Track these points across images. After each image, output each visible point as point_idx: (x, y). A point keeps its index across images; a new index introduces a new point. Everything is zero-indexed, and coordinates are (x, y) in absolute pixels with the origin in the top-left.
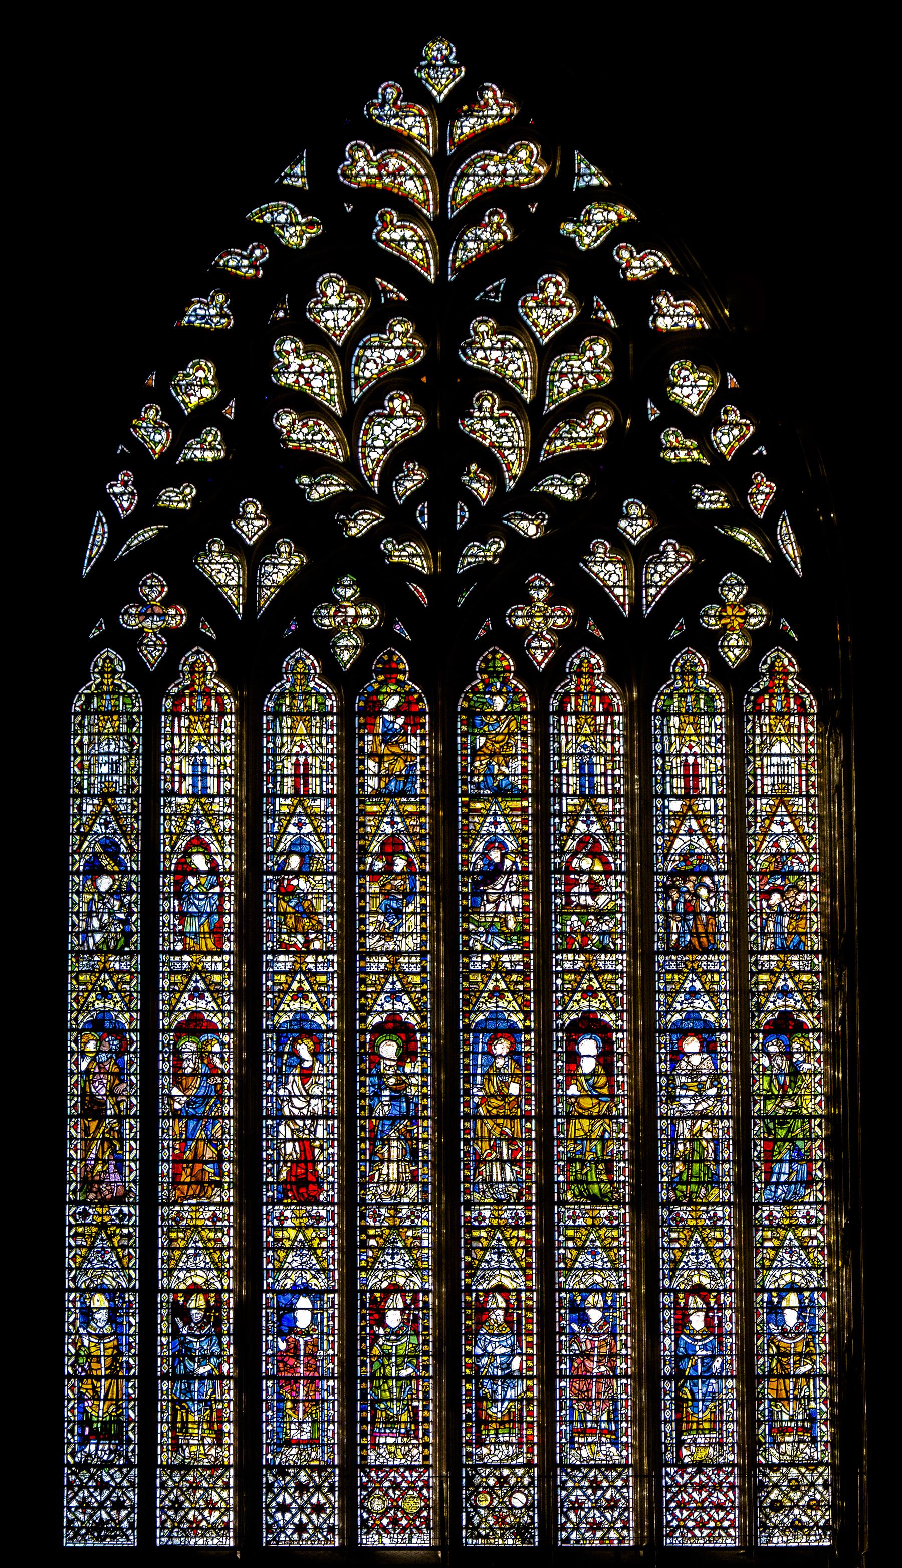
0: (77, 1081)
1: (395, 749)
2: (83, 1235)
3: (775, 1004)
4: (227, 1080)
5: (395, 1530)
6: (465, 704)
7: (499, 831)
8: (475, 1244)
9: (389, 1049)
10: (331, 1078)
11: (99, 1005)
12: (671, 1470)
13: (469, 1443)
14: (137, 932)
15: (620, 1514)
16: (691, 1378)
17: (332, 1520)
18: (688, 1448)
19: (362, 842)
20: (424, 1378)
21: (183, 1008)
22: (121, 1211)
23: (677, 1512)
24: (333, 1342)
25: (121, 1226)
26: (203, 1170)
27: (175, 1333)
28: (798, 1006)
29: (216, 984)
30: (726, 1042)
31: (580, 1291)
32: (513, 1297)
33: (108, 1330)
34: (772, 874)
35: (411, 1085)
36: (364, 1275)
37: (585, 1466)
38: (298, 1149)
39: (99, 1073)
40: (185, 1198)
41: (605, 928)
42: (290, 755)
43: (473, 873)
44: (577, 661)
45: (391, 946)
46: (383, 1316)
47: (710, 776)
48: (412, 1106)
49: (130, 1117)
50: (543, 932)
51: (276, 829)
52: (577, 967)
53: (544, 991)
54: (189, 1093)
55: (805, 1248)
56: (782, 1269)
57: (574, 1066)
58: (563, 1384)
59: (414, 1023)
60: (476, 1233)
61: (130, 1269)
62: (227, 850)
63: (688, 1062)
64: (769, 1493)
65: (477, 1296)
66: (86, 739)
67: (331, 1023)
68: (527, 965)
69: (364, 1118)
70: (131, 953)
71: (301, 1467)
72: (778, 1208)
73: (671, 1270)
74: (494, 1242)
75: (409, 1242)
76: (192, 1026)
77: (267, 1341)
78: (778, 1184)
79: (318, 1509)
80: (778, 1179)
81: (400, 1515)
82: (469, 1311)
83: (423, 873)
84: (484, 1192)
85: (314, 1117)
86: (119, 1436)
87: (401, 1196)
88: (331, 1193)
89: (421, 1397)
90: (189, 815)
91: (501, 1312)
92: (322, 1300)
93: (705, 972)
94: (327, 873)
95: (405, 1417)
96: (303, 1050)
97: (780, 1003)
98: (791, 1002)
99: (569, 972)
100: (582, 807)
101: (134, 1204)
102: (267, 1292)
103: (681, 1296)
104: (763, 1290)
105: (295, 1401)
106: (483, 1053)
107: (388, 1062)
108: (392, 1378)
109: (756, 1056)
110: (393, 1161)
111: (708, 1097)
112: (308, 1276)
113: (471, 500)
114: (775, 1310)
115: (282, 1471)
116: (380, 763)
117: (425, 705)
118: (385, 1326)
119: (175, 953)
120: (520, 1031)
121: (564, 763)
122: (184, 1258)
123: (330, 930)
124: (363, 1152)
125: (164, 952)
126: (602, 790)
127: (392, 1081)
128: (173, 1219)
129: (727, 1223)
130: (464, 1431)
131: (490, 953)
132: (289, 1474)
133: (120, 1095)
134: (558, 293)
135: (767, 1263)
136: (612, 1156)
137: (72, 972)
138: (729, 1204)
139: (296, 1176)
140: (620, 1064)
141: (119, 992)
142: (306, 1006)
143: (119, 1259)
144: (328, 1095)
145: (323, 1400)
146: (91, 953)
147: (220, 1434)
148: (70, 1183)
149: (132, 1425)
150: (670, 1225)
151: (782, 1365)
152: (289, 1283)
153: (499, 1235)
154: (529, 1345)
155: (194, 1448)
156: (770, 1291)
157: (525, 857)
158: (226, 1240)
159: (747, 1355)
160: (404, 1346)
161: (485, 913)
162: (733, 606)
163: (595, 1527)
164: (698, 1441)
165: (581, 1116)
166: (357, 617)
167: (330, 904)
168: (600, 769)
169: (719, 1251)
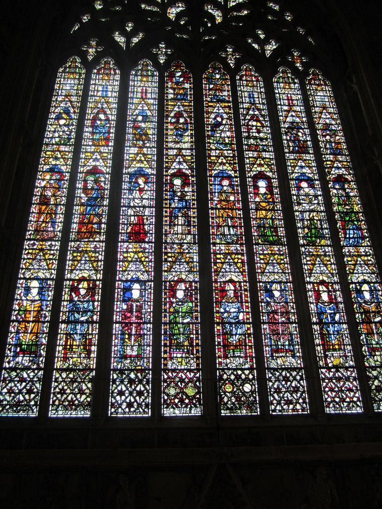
0: (39, 190)
2: (31, 254)
4: (106, 192)
5: (182, 406)
6: (205, 76)
7: (220, 111)
8: (218, 261)
9: (178, 182)
10: (152, 192)
11: (54, 163)
12: (324, 370)
13: (220, 357)
14: (73, 138)
15: (301, 395)
16: (326, 323)
17: (147, 400)
18: (330, 359)
19: (167, 113)
20: (195, 323)
21: (90, 164)
22: (51, 244)
23: (329, 393)
24: (150, 305)
25: (50, 250)
26: (92, 227)
27: (71, 300)
28: (344, 173)
29: (105, 157)
30: (318, 184)
31: (269, 282)
32: (237, 285)
33: (37, 298)
35: (187, 195)
36: (166, 274)
37: (280, 369)
38: (136, 219)
39: (50, 187)
40: (83, 239)
41: (264, 144)
42: (140, 86)
43: (211, 124)
44: (245, 67)
45: (178, 146)
46: (176, 293)
47: (297, 100)
48: (188, 204)
49: (60, 205)
50: (240, 144)
51: (133, 108)
52: (254, 156)
53: (242, 164)
54: (89, 196)
55: (367, 265)
56: (358, 273)
57: (256, 191)
58: (265, 326)
59: (188, 173)
60: (218, 256)
61: (51, 269)
62: (113, 113)
63: (304, 191)
64: (373, 382)
65: (221, 284)
67: (153, 172)
68: (234, 155)
69: (167, 208)
70: (70, 145)
71: (132, 370)
72: (351, 248)
73: (309, 273)
74: (227, 260)
75: (187, 259)
76: (93, 171)
77: (117, 305)
79: (140, 393)
80: (349, 236)
81: (184, 397)
82: (217, 291)
83: (191, 123)
84: (221, 239)
85: (144, 207)
86: (35, 353)
87: (183, 240)
89: (194, 333)
90: (100, 102)
91: (232, 292)
92: (145, 285)
93: (306, 160)
94: (153, 122)
95: (186, 343)
96: (141, 181)
97: (337, 171)
98: (341, 171)
99: (251, 157)
100: (251, 106)
101: (58, 241)
102: (118, 281)
104: (352, 283)
106: (218, 185)
107: (177, 187)
108: (179, 323)
109: (331, 189)
110: (180, 225)
111: (314, 204)
112: (139, 274)
114: (359, 292)
115: (121, 372)
116: (174, 91)
118: (176, 298)
119: (89, 145)
120: (233, 177)
121: (243, 94)
122: (79, 265)
123: (154, 140)
124: (166, 221)
125: (84, 145)
127: (179, 194)
128: (76, 248)
129: (331, 254)
130: (217, 350)
131: (219, 150)
132: (125, 374)
133: (58, 196)
135: (351, 271)
136: (277, 225)
137: (44, 150)
139: (135, 230)
140: (276, 191)
141: (64, 158)
142: (142, 165)
143: (48, 265)
144: (151, 198)
145: (144, 334)
146: (53, 144)
147: (89, 352)
148: (29, 231)
149: (43, 347)
150: (306, 254)
151: (368, 318)
152: (129, 277)
153: (229, 257)
154: (247, 307)
155: (75, 359)
156: (355, 283)
157: (231, 120)
158: (100, 257)
159: (350, 312)
160: (184, 308)
161: (216, 137)
163: (289, 402)
164: (334, 355)
165: (262, 210)
167: (154, 132)
169: (329, 266)
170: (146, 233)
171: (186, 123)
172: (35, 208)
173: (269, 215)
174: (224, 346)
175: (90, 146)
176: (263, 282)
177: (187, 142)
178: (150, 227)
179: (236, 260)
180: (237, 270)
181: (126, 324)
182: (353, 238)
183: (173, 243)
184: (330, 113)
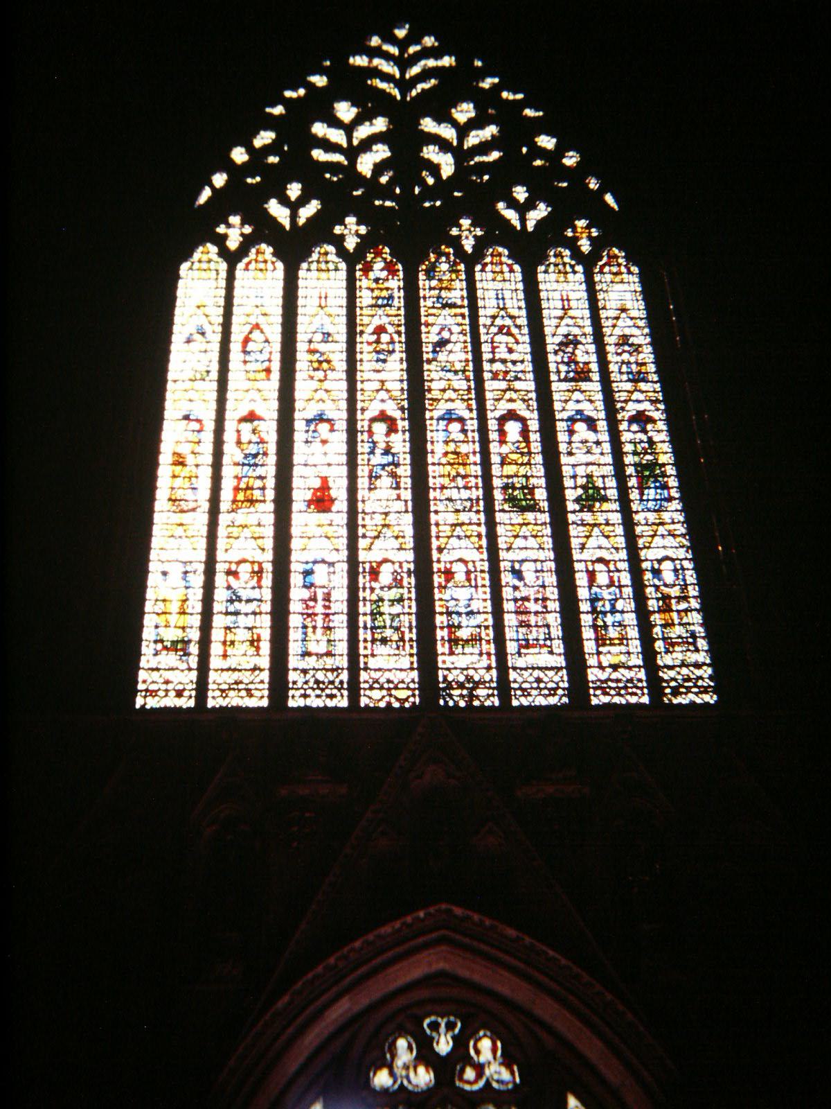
1: (381, 286)
3: (632, 408)
9: (380, 428)
13: (443, 654)
16: (601, 612)
20: (409, 614)
27: (229, 587)
31: (518, 561)
32: (470, 566)
48: (396, 459)
68: (469, 387)
74: (455, 534)
76: (249, 418)
78: (648, 500)
88: (341, 505)
103: (589, 563)
106: (443, 430)
113: (423, 183)
114: (657, 573)
115: (305, 672)
117: (400, 267)
127: (382, 445)
135: (647, 545)
138: (616, 511)
147: (258, 648)
149: (193, 643)
151: (666, 604)
156: (652, 561)
157: (465, 335)
160: (394, 594)
165: (510, 464)
170: (332, 501)
171: (392, 342)
173: (522, 470)
174: (450, 641)
177: (395, 368)
178: (339, 491)
180: (472, 546)
181: (309, 615)
182: (655, 500)
183: (374, 513)
184: (632, 318)
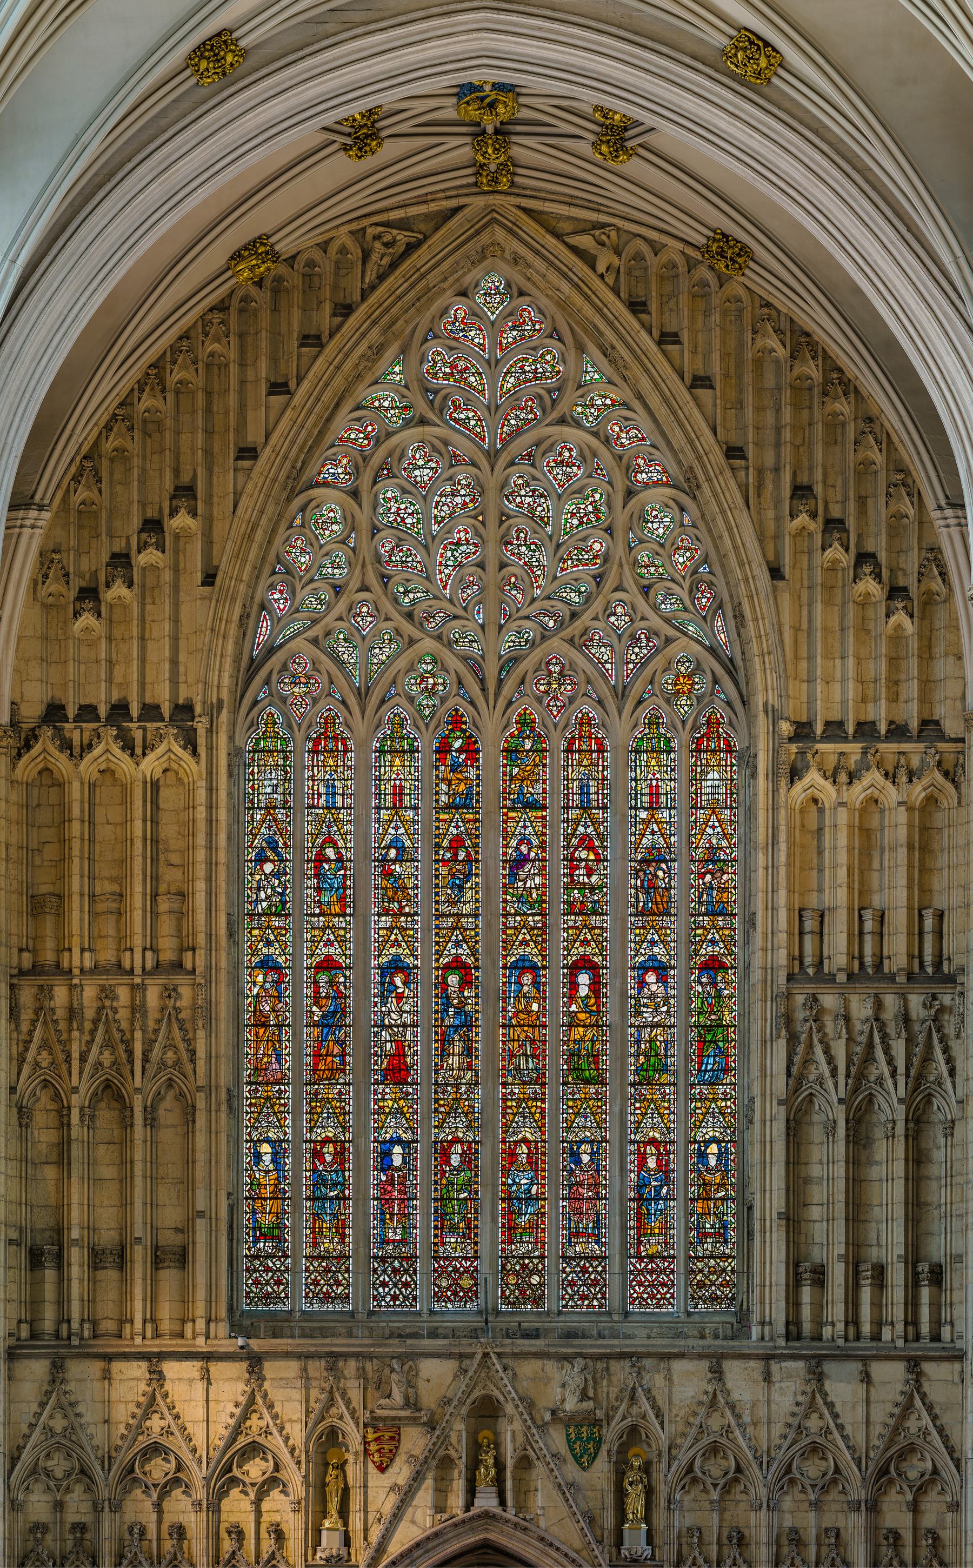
1: (459, 776)
2: (255, 1104)
11: (265, 950)
12: (634, 1261)
16: (647, 1199)
25: (279, 1098)
33: (271, 1167)
34: (707, 861)
40: (322, 1079)
45: (455, 910)
46: (450, 1158)
55: (723, 1114)
60: (509, 1104)
66: (256, 770)
71: (396, 1258)
78: (706, 1071)
85: (405, 1026)
93: (661, 928)
95: (462, 1225)
96: (398, 981)
105: (392, 1214)
115: (383, 1259)
116: (449, 785)
118: (450, 1165)
119: (314, 915)
126: (595, 804)
131: (520, 915)
134: (571, 456)
142: (400, 951)
143: (279, 1121)
146: (260, 915)
147: (343, 1236)
156: (699, 1142)
157: (544, 851)
162: (684, 677)
165: (578, 1025)
166: (435, 684)
168: (593, 790)
172: (250, 1032)
175: (318, 915)
176: (568, 1142)
179: (533, 1110)
183: (447, 1085)
